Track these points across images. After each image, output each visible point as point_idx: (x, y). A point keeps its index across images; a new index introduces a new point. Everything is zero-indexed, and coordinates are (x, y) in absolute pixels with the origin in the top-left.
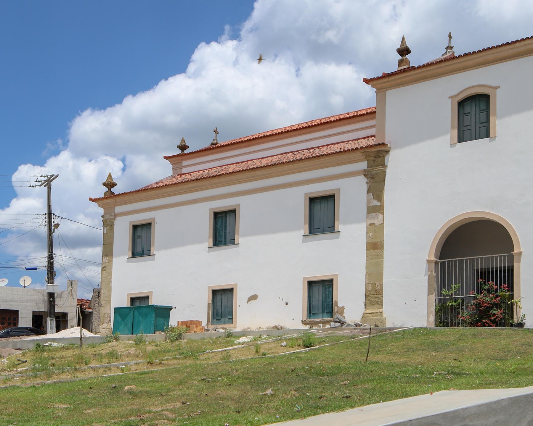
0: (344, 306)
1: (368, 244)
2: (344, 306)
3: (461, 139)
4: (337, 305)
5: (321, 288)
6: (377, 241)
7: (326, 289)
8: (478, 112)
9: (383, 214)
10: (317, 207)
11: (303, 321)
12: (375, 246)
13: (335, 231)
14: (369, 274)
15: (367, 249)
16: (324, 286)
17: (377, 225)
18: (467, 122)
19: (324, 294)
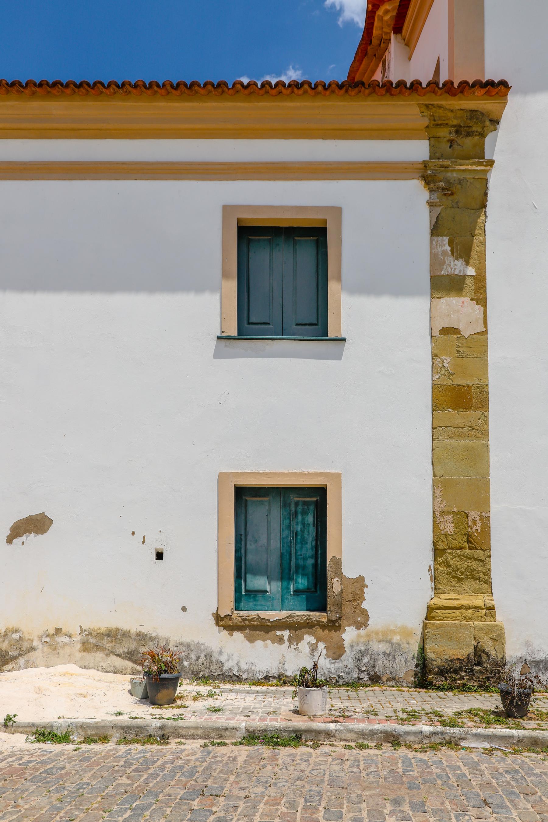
0: (362, 578)
1: (436, 388)
2: (362, 578)
4: (339, 573)
5: (276, 512)
7: (292, 517)
9: (485, 305)
10: (261, 256)
11: (218, 619)
12: (460, 399)
13: (331, 335)
14: (441, 483)
15: (435, 408)
16: (285, 505)
19: (286, 532)
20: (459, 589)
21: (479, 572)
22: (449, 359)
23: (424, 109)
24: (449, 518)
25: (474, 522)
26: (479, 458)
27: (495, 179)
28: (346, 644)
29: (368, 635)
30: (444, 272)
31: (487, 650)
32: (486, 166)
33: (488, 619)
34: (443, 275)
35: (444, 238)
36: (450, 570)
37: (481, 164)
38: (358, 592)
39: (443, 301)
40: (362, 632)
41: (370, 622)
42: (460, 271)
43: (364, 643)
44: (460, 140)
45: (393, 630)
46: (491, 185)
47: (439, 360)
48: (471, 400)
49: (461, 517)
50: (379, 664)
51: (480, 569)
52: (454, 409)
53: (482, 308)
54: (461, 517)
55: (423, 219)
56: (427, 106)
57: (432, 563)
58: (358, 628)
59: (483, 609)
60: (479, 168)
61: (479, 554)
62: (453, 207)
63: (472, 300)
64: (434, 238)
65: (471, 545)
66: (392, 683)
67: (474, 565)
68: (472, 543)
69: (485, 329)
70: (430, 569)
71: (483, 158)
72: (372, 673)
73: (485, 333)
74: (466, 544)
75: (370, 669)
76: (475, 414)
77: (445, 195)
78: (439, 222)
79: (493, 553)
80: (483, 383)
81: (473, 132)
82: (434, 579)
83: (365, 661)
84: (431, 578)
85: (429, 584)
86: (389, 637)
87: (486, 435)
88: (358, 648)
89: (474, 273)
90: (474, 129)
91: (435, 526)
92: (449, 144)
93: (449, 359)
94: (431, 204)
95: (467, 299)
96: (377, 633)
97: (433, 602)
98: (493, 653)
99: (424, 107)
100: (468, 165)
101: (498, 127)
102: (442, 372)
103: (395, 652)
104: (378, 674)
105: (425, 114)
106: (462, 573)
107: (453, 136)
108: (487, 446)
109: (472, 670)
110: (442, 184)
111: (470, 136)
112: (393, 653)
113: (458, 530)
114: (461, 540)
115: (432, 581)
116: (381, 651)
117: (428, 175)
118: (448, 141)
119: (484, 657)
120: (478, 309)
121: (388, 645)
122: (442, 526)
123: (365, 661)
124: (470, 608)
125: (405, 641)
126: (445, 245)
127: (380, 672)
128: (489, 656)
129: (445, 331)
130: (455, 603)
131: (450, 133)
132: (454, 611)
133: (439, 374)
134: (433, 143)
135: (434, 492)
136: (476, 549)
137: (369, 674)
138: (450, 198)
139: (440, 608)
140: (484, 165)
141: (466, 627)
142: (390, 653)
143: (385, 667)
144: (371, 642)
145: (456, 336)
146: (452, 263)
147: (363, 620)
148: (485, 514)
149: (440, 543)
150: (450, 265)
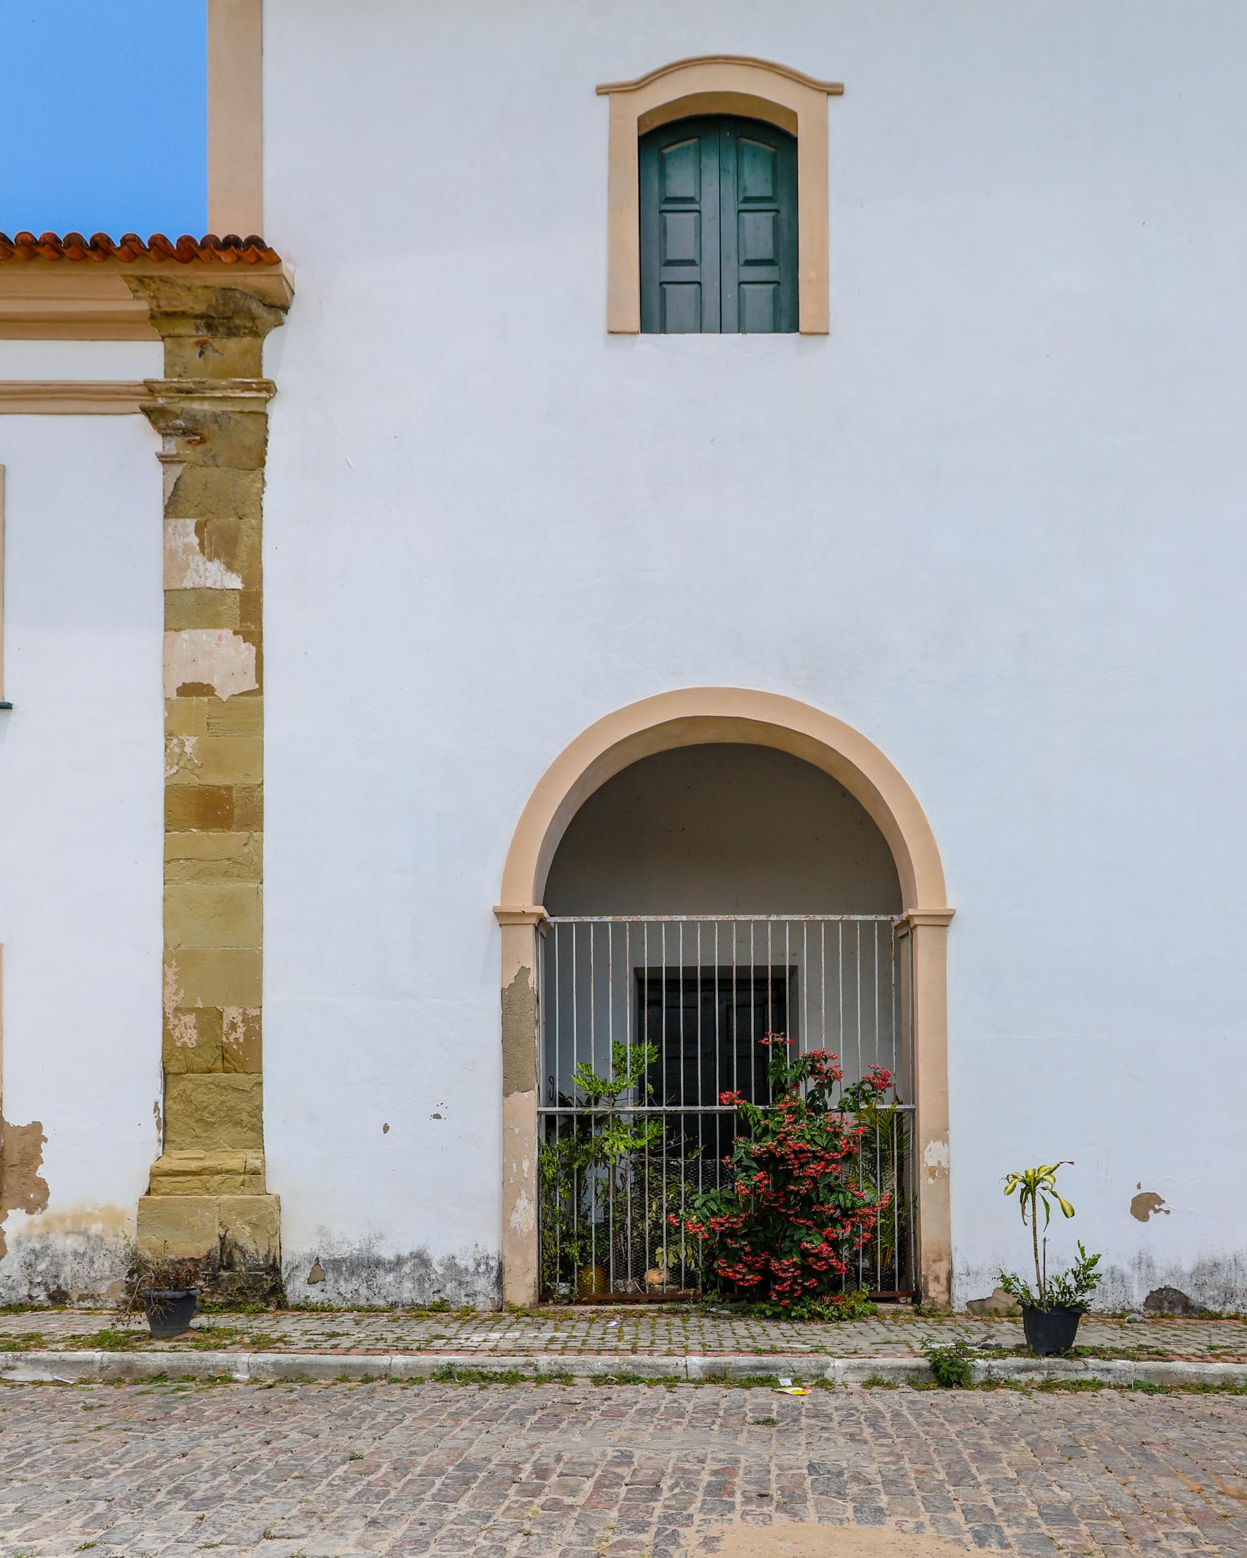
1: (173, 793)
3: (654, 319)
6: (226, 782)
8: (731, 205)
14: (179, 959)
17: (224, 693)
18: (681, 246)
20: (207, 1141)
21: (240, 1111)
22: (193, 740)
23: (135, 285)
24: (190, 1019)
25: (233, 1027)
26: (243, 914)
27: (278, 415)
28: (9, 1239)
29: (48, 1224)
30: (187, 584)
31: (240, 1243)
32: (259, 390)
33: (247, 1190)
34: (185, 590)
35: (188, 521)
36: (191, 1108)
37: (247, 387)
38: (31, 1150)
39: (184, 635)
40: (37, 1217)
41: (50, 1201)
42: (216, 582)
43: (41, 1237)
44: (217, 343)
45: (90, 1215)
46: (272, 424)
47: (175, 741)
48: (231, 812)
49: (210, 1019)
50: (66, 1272)
51: (242, 1105)
52: (202, 828)
53: (253, 649)
54: (210, 1019)
55: (152, 485)
56: (140, 280)
57: (160, 1098)
58: (30, 1212)
59: (240, 1174)
60: (247, 394)
61: (240, 1079)
62: (205, 465)
63: (235, 633)
64: (170, 520)
65: (226, 1064)
66: (88, 1304)
67: (232, 1099)
68: (229, 1062)
69: (257, 686)
70: (156, 1109)
71: (260, 375)
72: (53, 1288)
73: (259, 692)
74: (219, 1064)
75: (50, 1281)
76: (236, 836)
77: (190, 442)
78: (180, 493)
79: (267, 1078)
80: (253, 782)
81: (238, 327)
82: (164, 1125)
83: (42, 1266)
84: (158, 1123)
85: (153, 1134)
86: (84, 1226)
87: (258, 874)
88: (30, 1245)
89: (240, 586)
90: (237, 321)
91: (167, 1035)
92: (198, 350)
93: (193, 740)
94: (164, 459)
95: (227, 632)
96: (62, 1219)
97: (160, 1163)
98: (251, 1248)
99: (136, 282)
100: (225, 388)
101: (285, 318)
102: (182, 764)
103: (94, 1250)
104: (64, 1288)
105: (140, 294)
106: (212, 1114)
107: (203, 333)
108: (258, 894)
109: (215, 1278)
110: (180, 422)
111: (234, 335)
112: (90, 1253)
113: (204, 1039)
114: (209, 1056)
115: (159, 1129)
116: (69, 1250)
117: (156, 406)
118: (197, 343)
119: (237, 1255)
120: (247, 650)
121: (81, 1239)
122: (177, 1034)
123: (42, 1266)
124: (219, 1173)
125: (111, 1233)
126: (188, 534)
127: (67, 1285)
128: (243, 1253)
129: (188, 690)
130: (194, 1166)
131: (198, 329)
132: (189, 1178)
133: (176, 768)
134: (169, 347)
135: (164, 975)
136: (236, 1071)
137: (47, 1289)
138: (199, 448)
139: (166, 1174)
140: (254, 390)
141: (206, 1205)
142: (84, 1254)
143: (75, 1277)
144: (52, 1236)
145: (205, 699)
146: (202, 568)
147: (38, 1197)
148: (253, 1012)
149: (173, 1062)
150: (197, 571)
